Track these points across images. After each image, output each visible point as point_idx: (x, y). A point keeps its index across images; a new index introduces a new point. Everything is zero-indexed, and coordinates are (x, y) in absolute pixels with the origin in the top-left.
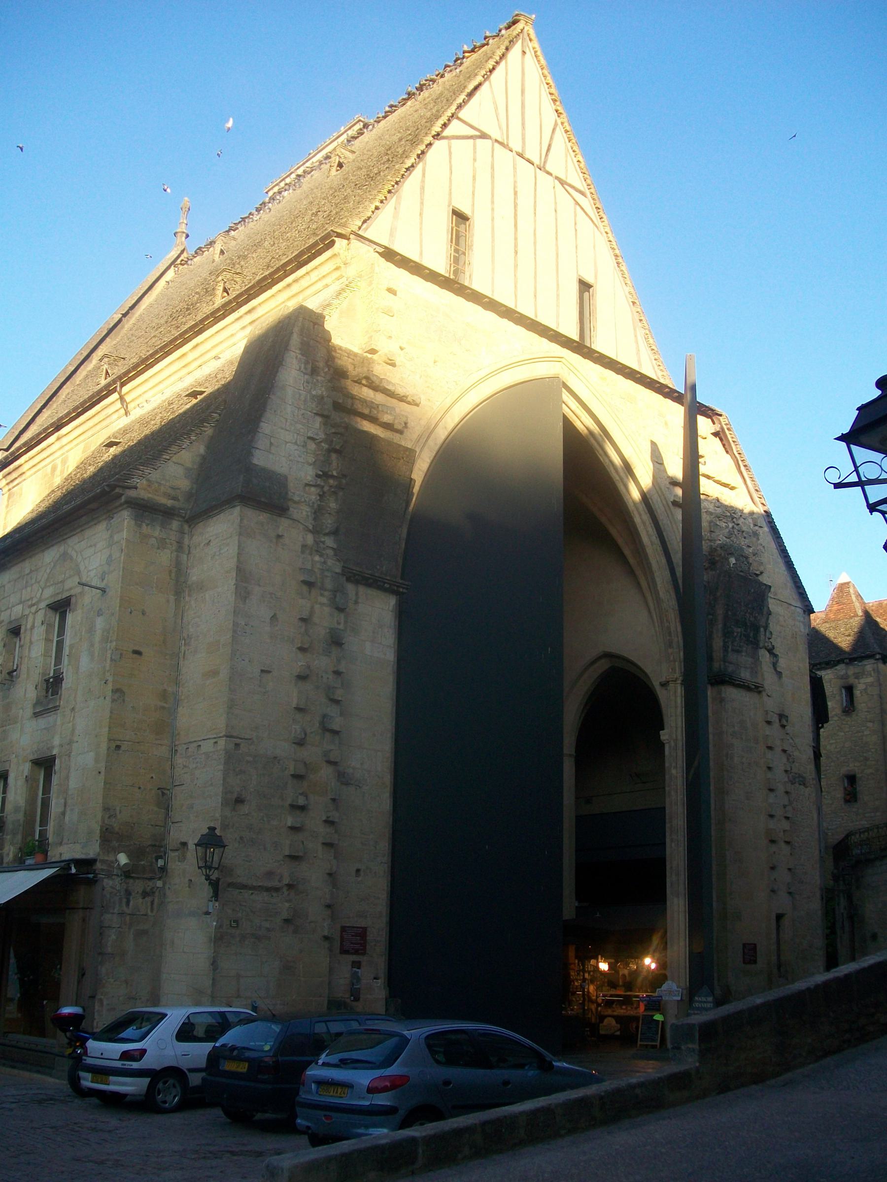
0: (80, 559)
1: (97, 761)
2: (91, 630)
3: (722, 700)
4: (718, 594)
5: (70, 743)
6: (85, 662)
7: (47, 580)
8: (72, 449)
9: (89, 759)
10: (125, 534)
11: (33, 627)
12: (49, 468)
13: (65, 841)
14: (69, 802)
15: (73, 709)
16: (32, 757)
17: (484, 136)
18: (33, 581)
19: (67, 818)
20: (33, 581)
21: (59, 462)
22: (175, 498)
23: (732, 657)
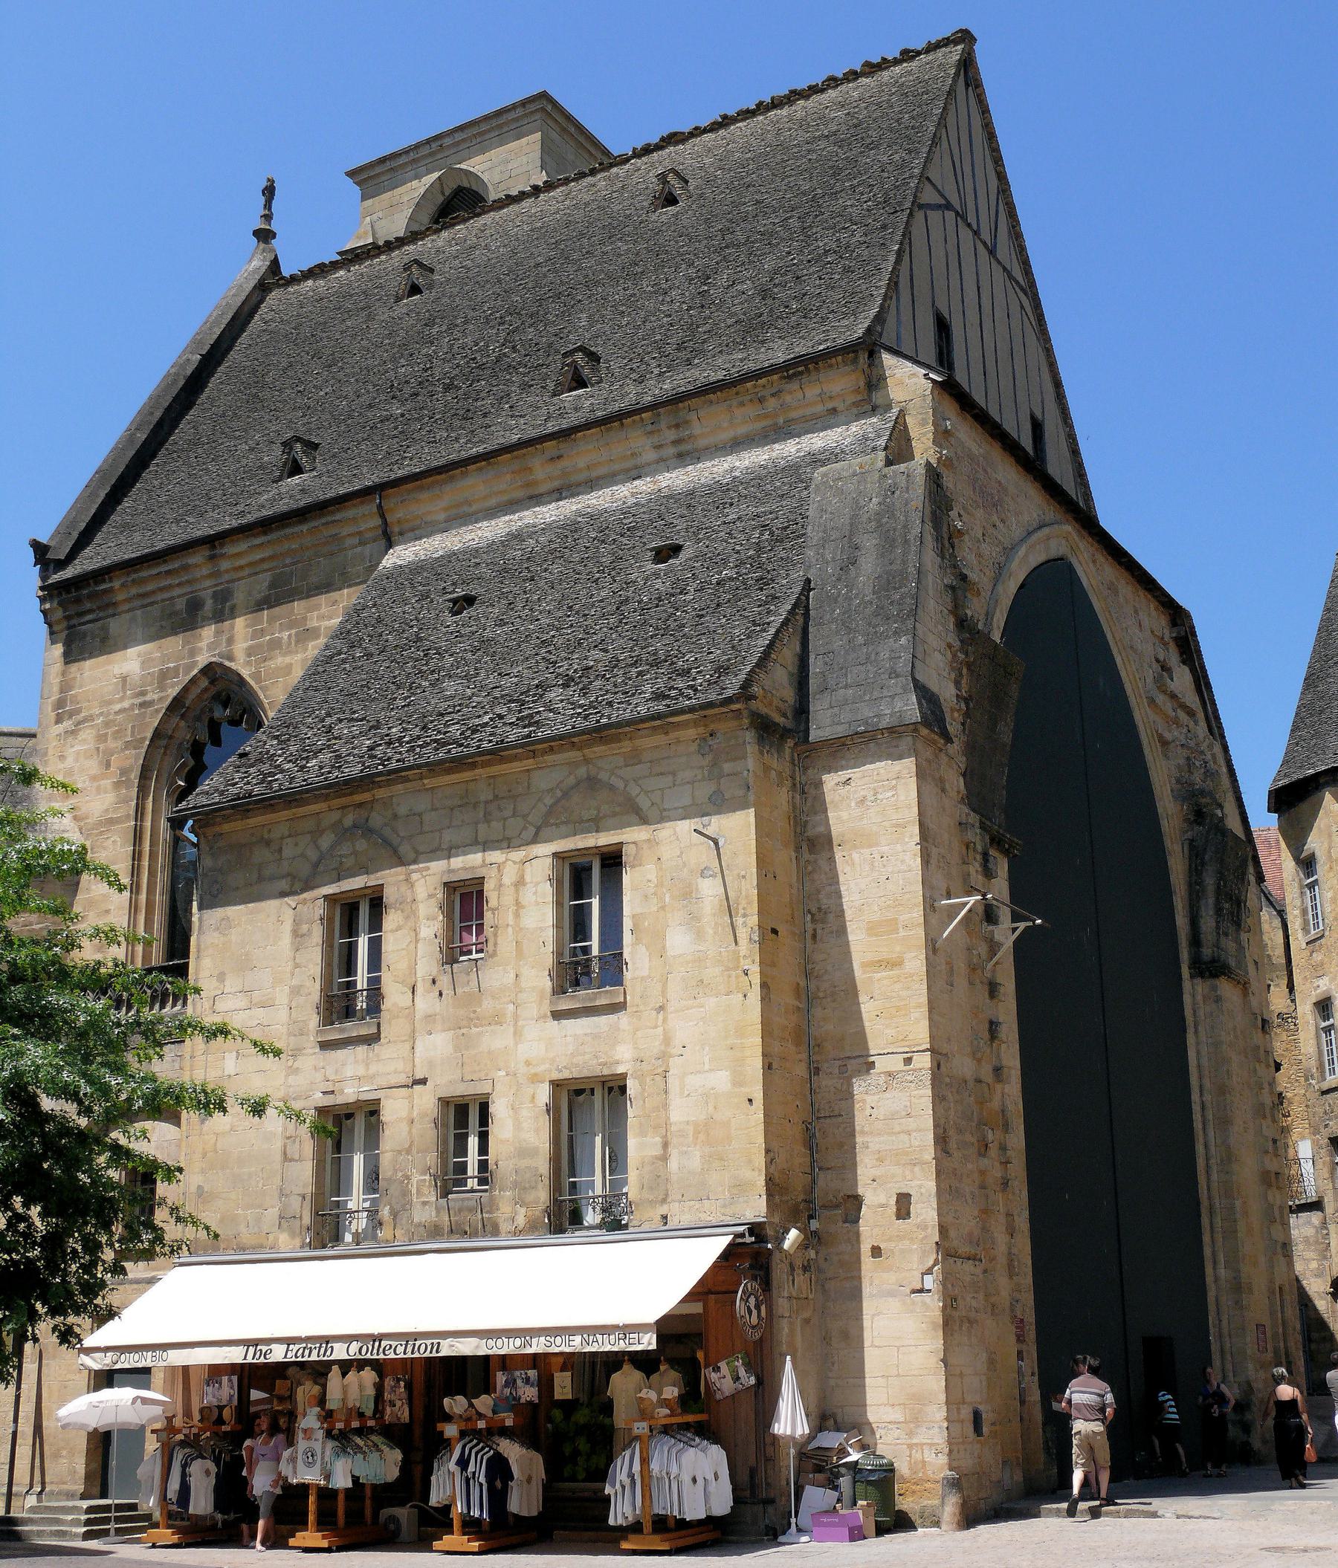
0: (634, 790)
1: (738, 1082)
2: (688, 894)
3: (1218, 1000)
4: (1207, 857)
5: (664, 1056)
6: (678, 941)
7: (550, 813)
8: (239, 579)
9: (721, 1080)
10: (751, 763)
11: (520, 883)
12: (181, 604)
13: (675, 1195)
14: (674, 1141)
15: (661, 1008)
16: (556, 1076)
17: (948, 206)
18: (508, 813)
19: (673, 1164)
20: (508, 813)
21: (207, 596)
22: (784, 715)
23: (1223, 940)
